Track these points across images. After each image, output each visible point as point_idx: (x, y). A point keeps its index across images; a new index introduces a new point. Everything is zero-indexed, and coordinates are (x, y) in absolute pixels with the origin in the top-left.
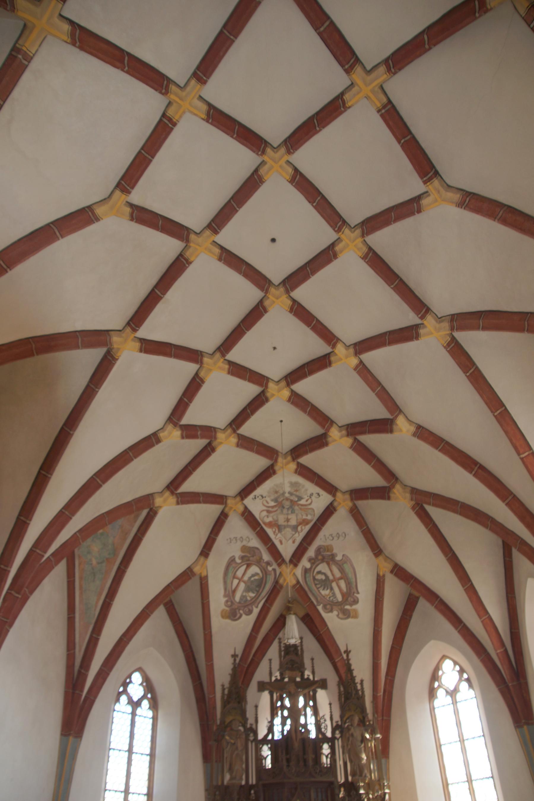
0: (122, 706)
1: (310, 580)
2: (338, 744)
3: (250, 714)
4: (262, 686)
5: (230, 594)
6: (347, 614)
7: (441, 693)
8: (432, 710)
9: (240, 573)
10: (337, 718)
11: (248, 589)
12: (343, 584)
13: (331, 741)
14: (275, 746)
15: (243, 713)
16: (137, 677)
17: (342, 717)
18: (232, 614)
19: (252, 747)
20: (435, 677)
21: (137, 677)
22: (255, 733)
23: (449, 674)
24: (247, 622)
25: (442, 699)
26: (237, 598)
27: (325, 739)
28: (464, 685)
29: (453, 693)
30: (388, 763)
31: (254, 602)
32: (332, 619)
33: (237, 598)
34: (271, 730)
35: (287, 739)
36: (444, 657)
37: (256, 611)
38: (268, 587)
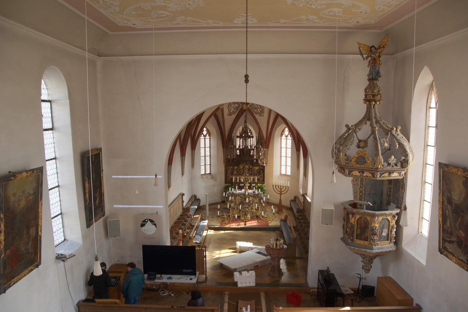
0: (202, 137)
1: (251, 108)
2: (255, 151)
3: (234, 144)
4: (238, 137)
5: (229, 111)
6: (261, 116)
7: (284, 135)
8: (281, 139)
9: (232, 106)
10: (255, 145)
11: (234, 109)
12: (260, 109)
14: (240, 150)
15: (233, 143)
16: (205, 129)
17: (257, 145)
18: (230, 114)
19: (235, 150)
20: (283, 131)
22: (236, 147)
23: (287, 132)
24: (234, 116)
25: (284, 137)
26: (231, 111)
27: (252, 149)
28: (289, 136)
29: (287, 136)
31: (236, 112)
32: (257, 116)
33: (231, 111)
35: (243, 149)
36: (286, 128)
38: (240, 108)
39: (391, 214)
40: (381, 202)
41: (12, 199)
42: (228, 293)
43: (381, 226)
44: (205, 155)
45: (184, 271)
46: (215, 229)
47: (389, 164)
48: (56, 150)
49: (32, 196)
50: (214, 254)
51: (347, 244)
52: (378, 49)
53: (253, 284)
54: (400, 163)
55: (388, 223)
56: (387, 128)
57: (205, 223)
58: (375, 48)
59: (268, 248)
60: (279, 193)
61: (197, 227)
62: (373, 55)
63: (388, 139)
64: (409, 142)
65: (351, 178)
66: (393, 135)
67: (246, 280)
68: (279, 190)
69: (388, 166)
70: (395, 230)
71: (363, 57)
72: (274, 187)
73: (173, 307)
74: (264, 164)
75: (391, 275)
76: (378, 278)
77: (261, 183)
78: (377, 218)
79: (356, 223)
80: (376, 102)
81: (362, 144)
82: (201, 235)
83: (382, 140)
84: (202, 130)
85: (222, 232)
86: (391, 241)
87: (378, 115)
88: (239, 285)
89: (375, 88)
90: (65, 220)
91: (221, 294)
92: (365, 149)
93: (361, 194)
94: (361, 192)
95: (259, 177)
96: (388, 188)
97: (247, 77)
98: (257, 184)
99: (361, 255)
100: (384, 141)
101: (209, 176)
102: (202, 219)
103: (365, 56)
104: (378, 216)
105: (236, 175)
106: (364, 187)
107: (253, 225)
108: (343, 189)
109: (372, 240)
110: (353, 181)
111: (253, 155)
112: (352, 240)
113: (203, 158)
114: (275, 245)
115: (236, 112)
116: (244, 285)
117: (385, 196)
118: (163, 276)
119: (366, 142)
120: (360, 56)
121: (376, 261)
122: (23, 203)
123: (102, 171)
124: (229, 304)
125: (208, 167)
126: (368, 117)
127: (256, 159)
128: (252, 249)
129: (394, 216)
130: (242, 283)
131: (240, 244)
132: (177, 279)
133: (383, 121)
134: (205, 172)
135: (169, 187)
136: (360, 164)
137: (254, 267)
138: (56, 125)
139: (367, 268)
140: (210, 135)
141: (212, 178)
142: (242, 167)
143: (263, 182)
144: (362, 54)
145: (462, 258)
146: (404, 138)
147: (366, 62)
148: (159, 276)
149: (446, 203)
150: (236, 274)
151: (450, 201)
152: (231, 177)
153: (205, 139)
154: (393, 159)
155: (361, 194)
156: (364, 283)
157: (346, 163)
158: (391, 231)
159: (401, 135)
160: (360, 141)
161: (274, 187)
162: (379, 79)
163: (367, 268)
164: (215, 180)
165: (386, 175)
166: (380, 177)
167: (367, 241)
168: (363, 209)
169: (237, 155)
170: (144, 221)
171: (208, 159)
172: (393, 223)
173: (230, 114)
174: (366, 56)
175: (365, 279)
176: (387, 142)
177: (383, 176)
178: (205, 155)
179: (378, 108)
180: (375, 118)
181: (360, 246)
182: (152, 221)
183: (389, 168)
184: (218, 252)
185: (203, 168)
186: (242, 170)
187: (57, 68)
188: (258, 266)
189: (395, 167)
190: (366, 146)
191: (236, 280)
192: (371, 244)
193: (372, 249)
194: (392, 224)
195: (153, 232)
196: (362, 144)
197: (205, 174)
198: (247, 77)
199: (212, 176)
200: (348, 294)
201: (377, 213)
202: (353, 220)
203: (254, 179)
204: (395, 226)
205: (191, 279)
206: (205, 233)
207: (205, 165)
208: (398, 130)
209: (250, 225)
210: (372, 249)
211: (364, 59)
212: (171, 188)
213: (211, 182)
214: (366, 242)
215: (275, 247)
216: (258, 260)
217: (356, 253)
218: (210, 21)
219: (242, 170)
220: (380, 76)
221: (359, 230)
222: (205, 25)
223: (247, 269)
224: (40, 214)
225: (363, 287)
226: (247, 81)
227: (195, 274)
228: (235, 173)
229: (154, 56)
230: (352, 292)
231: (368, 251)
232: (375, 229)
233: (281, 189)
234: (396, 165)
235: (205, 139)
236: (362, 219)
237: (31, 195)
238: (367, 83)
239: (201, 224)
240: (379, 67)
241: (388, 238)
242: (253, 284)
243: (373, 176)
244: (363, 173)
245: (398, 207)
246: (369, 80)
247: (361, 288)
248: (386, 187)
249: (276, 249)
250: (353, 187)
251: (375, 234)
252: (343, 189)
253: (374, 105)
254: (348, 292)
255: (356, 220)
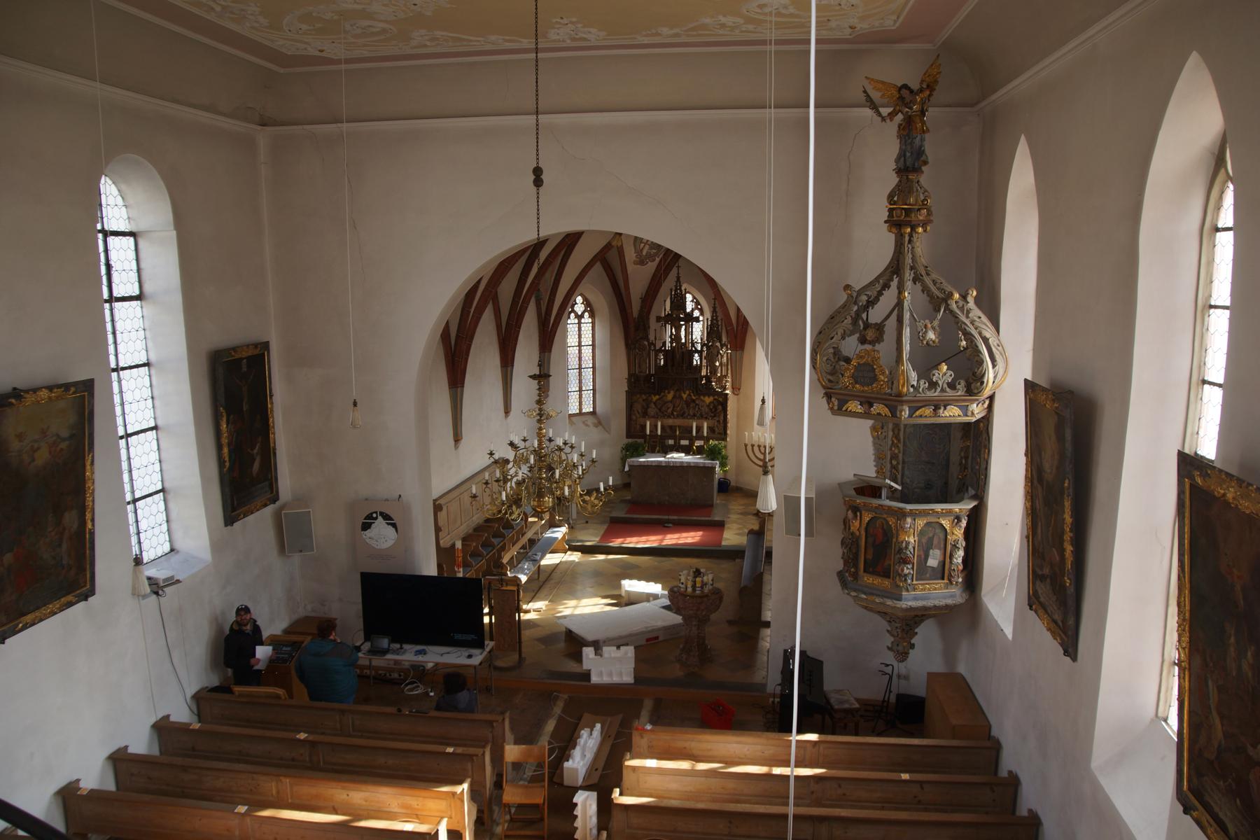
0: (573, 320)
2: (705, 354)
5: (639, 252)
13: (700, 353)
14: (666, 353)
16: (579, 299)
18: (641, 261)
19: (652, 354)
21: (579, 299)
24: (651, 267)
27: (696, 351)
30: (742, 358)
31: (656, 255)
34: (664, 344)
37: (658, 260)
39: (950, 512)
40: (946, 483)
41: (15, 445)
42: (566, 696)
43: (924, 541)
44: (580, 365)
45: (458, 637)
46: (586, 550)
47: (933, 385)
48: (150, 345)
49: (67, 443)
50: (561, 608)
51: (844, 584)
52: (917, 94)
53: (628, 678)
54: (963, 383)
55: (942, 535)
56: (937, 293)
57: (560, 533)
58: (911, 91)
59: (674, 594)
60: (761, 463)
61: (530, 540)
62: (909, 107)
63: (936, 323)
64: (998, 332)
65: (870, 422)
66: (951, 312)
67: (611, 668)
68: (761, 457)
69: (929, 389)
70: (961, 553)
71: (879, 114)
72: (749, 448)
73: (399, 710)
74: (725, 389)
75: (962, 669)
76: (929, 674)
77: (717, 439)
78: (909, 520)
79: (863, 533)
80: (913, 228)
81: (870, 334)
82: (535, 561)
83: (920, 325)
84: (568, 301)
85: (602, 557)
86: (951, 583)
87: (923, 261)
88: (595, 679)
89: (910, 191)
90: (171, 505)
91: (548, 697)
92: (877, 347)
93: (894, 462)
94: (894, 457)
95: (712, 422)
96: (962, 449)
97: (538, 172)
98: (707, 440)
99: (883, 614)
100: (926, 326)
101: (591, 420)
102: (552, 524)
103: (885, 111)
104: (914, 515)
105: (656, 417)
106: (901, 446)
107: (681, 542)
108: (854, 449)
109: (900, 575)
110: (873, 429)
111: (699, 368)
112: (855, 576)
113: (573, 375)
114: (689, 585)
115: (656, 255)
116: (606, 680)
117: (954, 469)
118: (406, 646)
119: (880, 328)
120: (868, 112)
121: (926, 634)
122: (43, 456)
123: (271, 396)
124: (560, 720)
125: (588, 396)
126: (895, 268)
127: (706, 376)
128: (656, 597)
129: (958, 519)
130: (601, 674)
131: (632, 586)
132: (437, 656)
133: (934, 276)
134: (580, 409)
135: (457, 439)
136: (862, 385)
137: (648, 640)
138: (148, 288)
139: (900, 648)
140: (592, 315)
141: (599, 423)
142: (670, 397)
143: (723, 435)
144: (874, 106)
145: (1056, 617)
146: (984, 319)
147: (892, 128)
148: (398, 646)
149: (1035, 482)
150: (588, 652)
151: (1040, 480)
152: (641, 420)
153: (579, 323)
154: (944, 373)
155: (894, 462)
156: (899, 687)
157: (830, 381)
158: (951, 556)
159: (976, 312)
160: (867, 326)
161: (749, 448)
162: (924, 168)
163: (900, 648)
164: (607, 430)
165: (928, 411)
166: (911, 416)
167: (888, 577)
168: (880, 497)
169: (658, 367)
170: (370, 517)
171: (588, 374)
172: (958, 534)
173: (641, 261)
174: (891, 110)
175: (906, 678)
176: (933, 328)
177: (917, 413)
178: (580, 365)
179: (922, 245)
180: (912, 268)
181: (871, 591)
182: (386, 517)
183: (930, 394)
184: (572, 603)
185: (574, 398)
186: (670, 405)
187: (141, 159)
188: (657, 638)
189: (950, 392)
190: (879, 339)
191: (586, 665)
192: (898, 586)
193: (899, 598)
194: (954, 537)
195: (390, 543)
196: (870, 334)
197: (581, 414)
198: (538, 172)
199: (598, 418)
200: (846, 711)
201: (909, 507)
202: (857, 524)
203: (699, 429)
204: (962, 543)
205: (470, 656)
206: (550, 560)
207: (580, 390)
208: (970, 299)
209: (674, 542)
210: (899, 598)
211: (883, 119)
212: (463, 443)
213: (596, 434)
214: (887, 582)
215: (690, 590)
216: (660, 624)
217: (866, 608)
218: (493, 38)
219: (670, 405)
220: (925, 163)
221: (871, 551)
222: (488, 47)
223: (619, 642)
224: (89, 484)
225: (899, 696)
226: (538, 182)
227: (481, 645)
228: (652, 410)
229: (345, 125)
230: (857, 706)
231: (889, 602)
232: (907, 548)
233: (764, 454)
234: (952, 386)
235: (579, 323)
236: (878, 523)
237: (64, 440)
238: (893, 180)
239: (548, 534)
240: (922, 140)
241: (942, 572)
242: (628, 678)
243: (894, 415)
244: (871, 405)
245: (974, 497)
246: (899, 171)
247: (893, 699)
248: (956, 445)
249: (692, 597)
250: (874, 444)
251: (905, 561)
252: (854, 449)
253: (911, 236)
254: (846, 706)
255: (864, 526)
